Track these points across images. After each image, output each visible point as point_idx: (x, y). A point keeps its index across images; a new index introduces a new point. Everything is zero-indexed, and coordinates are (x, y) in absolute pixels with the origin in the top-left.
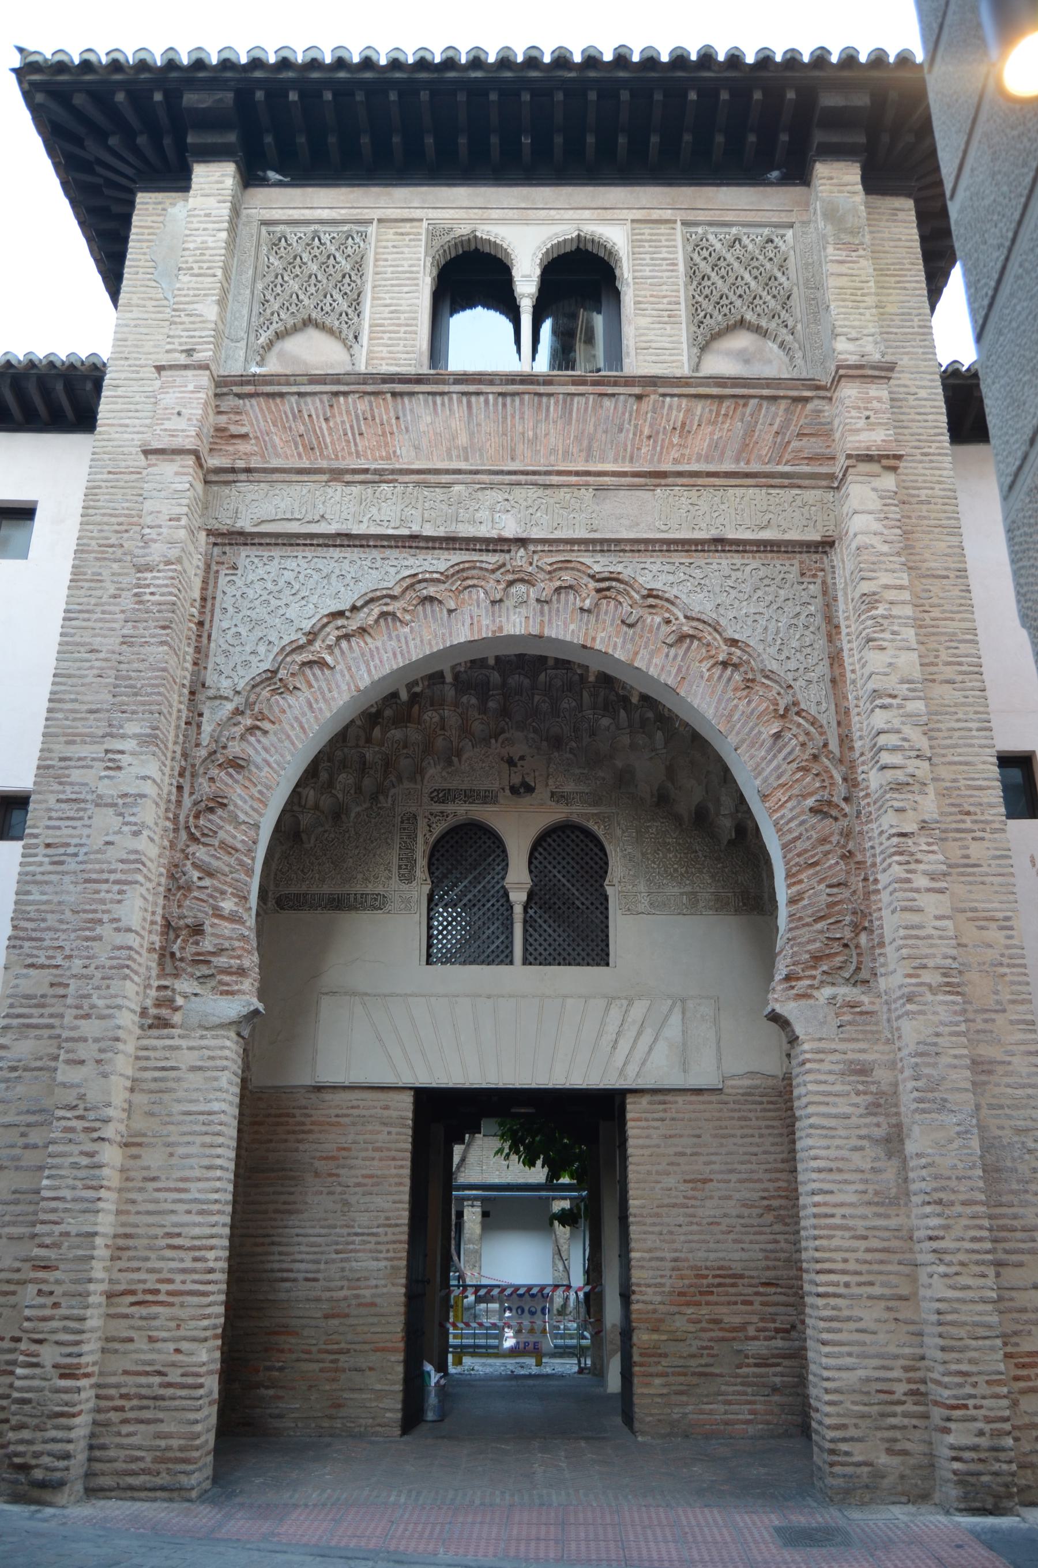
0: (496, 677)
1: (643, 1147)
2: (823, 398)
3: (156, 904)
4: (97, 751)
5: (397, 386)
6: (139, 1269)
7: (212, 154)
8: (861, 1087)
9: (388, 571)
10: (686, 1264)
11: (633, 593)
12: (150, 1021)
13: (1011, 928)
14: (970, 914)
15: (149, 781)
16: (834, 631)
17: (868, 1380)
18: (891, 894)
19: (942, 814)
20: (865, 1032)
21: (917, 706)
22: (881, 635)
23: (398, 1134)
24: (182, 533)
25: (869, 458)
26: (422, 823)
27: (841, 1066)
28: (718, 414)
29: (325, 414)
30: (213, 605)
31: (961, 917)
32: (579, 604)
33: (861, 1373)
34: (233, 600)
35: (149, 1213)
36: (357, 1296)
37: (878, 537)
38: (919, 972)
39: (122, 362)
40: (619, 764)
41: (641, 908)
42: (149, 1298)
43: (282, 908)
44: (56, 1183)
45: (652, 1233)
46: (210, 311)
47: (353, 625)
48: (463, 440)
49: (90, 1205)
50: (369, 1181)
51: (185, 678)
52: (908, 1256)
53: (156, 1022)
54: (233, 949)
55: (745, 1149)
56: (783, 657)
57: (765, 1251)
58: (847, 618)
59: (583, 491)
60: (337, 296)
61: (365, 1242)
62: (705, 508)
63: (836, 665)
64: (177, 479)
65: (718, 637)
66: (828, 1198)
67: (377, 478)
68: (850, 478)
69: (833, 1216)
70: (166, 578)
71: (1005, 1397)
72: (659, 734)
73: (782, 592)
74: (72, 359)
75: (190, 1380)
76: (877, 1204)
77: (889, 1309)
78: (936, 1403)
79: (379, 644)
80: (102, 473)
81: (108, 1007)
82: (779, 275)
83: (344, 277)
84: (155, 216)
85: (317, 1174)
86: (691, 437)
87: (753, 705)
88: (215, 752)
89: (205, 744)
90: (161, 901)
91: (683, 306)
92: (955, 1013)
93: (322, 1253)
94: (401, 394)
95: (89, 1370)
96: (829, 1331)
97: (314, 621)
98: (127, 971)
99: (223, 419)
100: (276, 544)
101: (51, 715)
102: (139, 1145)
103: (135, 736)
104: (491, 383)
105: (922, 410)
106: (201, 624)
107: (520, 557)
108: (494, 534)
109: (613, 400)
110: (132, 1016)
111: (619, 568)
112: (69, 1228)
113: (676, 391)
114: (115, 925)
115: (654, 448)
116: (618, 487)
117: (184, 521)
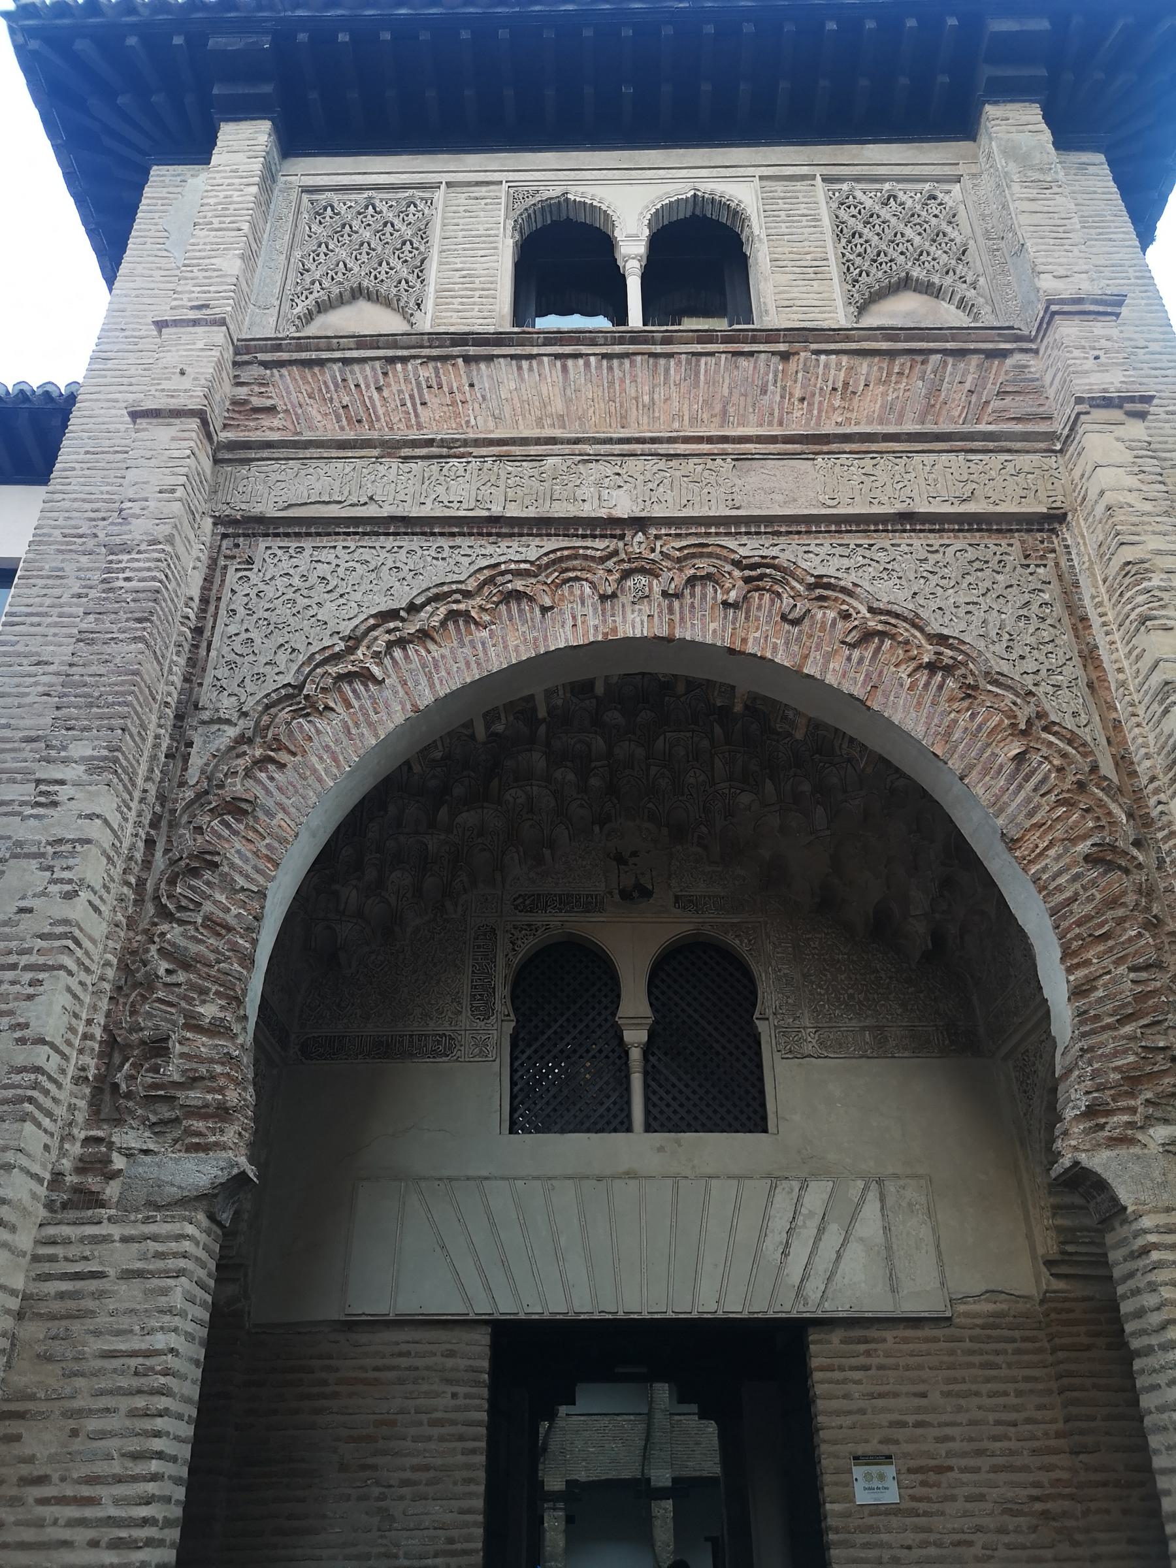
1: (838, 1413)
3: (95, 1008)
9: (463, 561)
15: (98, 822)
16: (1080, 626)
22: (1163, 613)
23: (467, 1396)
24: (177, 507)
25: (1106, 402)
28: (889, 375)
29: (376, 381)
30: (217, 608)
32: (720, 597)
34: (246, 599)
39: (117, 334)
41: (808, 1049)
46: (232, 265)
48: (558, 406)
51: (169, 694)
53: (76, 1197)
54: (213, 1077)
55: (997, 1416)
56: (1014, 656)
59: (719, 461)
64: (175, 445)
65: (918, 634)
67: (444, 451)
68: (1081, 431)
70: (148, 560)
72: (820, 810)
73: (1000, 578)
82: (949, 230)
83: (404, 243)
84: (173, 198)
85: (343, 1467)
86: (857, 398)
87: (979, 719)
88: (207, 793)
89: (192, 782)
90: (104, 1004)
91: (832, 261)
97: (356, 622)
98: (28, 1107)
99: (242, 392)
100: (308, 535)
102: (20, 1416)
103: (84, 760)
105: (1158, 365)
106: (198, 631)
107: (638, 542)
108: (603, 513)
109: (752, 360)
110: (33, 1185)
111: (774, 552)
114: (18, 1034)
116: (765, 457)
117: (178, 494)
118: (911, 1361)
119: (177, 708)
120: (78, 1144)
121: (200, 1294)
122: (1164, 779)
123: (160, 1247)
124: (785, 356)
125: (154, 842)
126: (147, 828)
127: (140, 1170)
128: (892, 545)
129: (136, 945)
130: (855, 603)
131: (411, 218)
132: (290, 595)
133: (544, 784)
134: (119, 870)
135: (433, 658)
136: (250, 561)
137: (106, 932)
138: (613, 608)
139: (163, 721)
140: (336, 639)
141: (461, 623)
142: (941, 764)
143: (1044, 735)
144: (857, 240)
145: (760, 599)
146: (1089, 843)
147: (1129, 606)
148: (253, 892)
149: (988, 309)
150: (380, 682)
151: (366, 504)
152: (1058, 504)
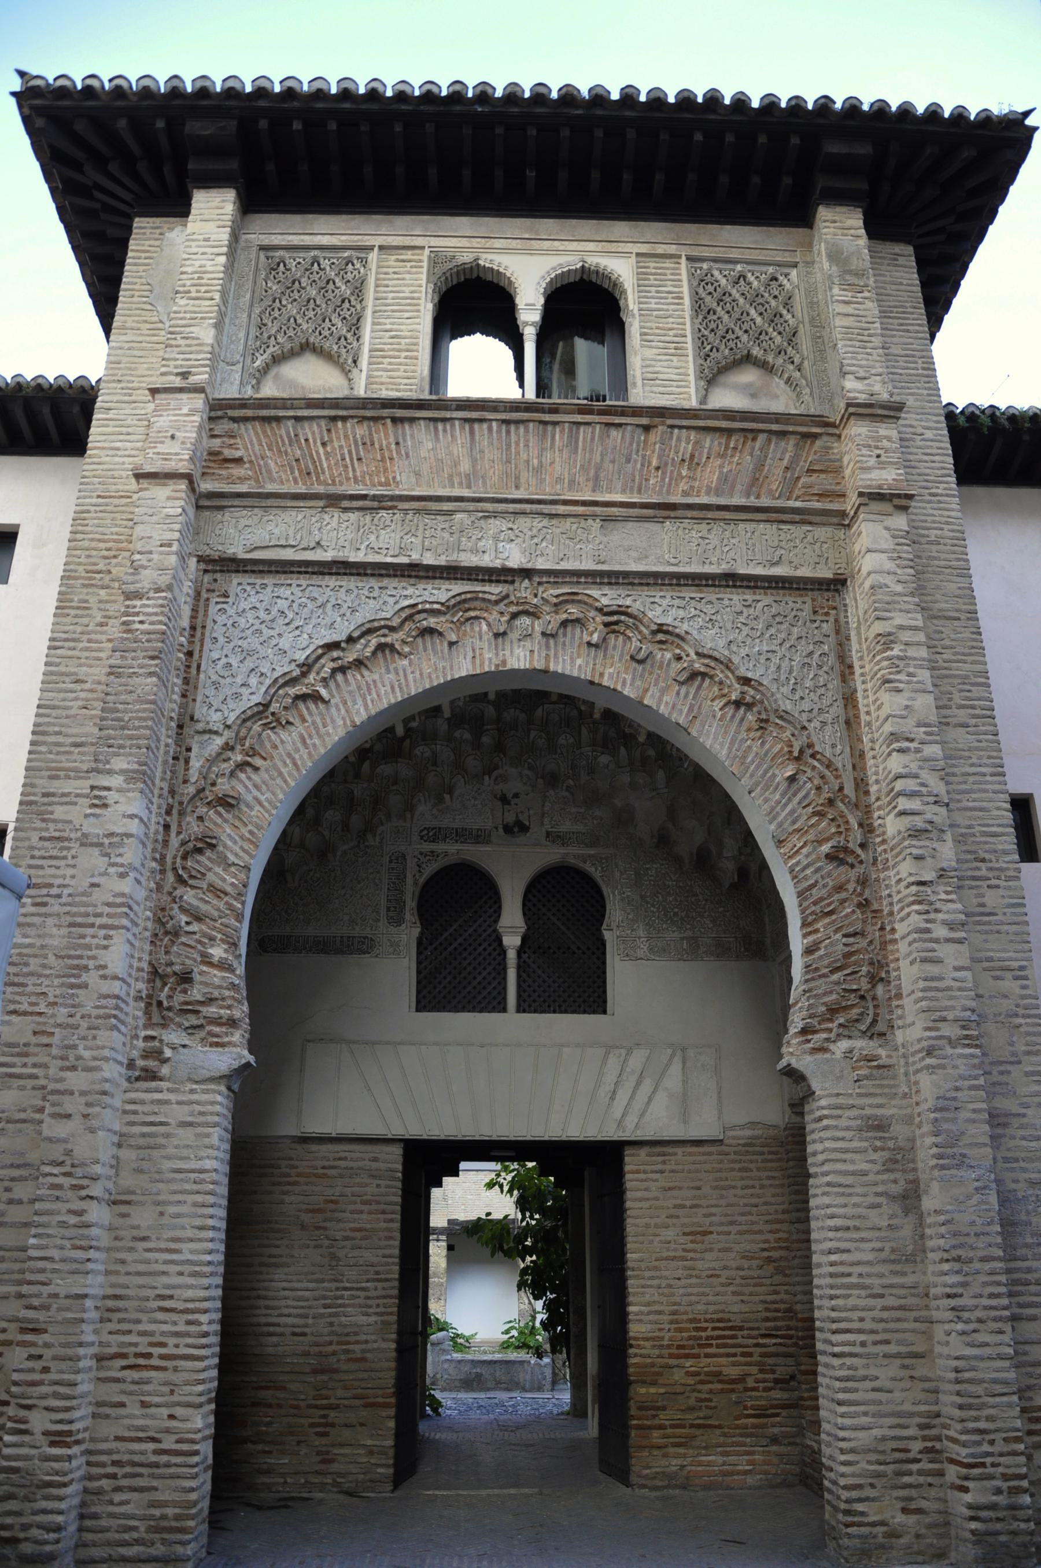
0: (490, 711)
1: (641, 1200)
2: (832, 435)
4: (83, 786)
5: (398, 412)
6: (130, 1332)
7: (212, 181)
8: (878, 1143)
10: (685, 1317)
11: (642, 628)
12: (137, 1074)
13: (1026, 978)
14: (986, 964)
15: (137, 820)
16: (847, 671)
17: (884, 1439)
18: (910, 944)
19: (958, 861)
20: (882, 1086)
21: (933, 750)
22: (898, 677)
23: (387, 1187)
24: (173, 559)
26: (411, 863)
27: (859, 1122)
28: (727, 448)
29: (322, 438)
30: (203, 634)
31: (978, 967)
32: (586, 638)
33: (876, 1432)
35: (139, 1274)
36: (347, 1352)
37: (891, 577)
38: (940, 1025)
39: (115, 385)
40: (618, 803)
41: (640, 953)
42: (141, 1361)
43: (265, 951)
44: (43, 1242)
45: (651, 1286)
46: (207, 334)
47: (351, 657)
48: (465, 466)
49: (78, 1266)
50: (358, 1235)
51: (173, 710)
52: (923, 1313)
53: (143, 1074)
54: (223, 999)
56: (797, 697)
57: (765, 1302)
58: (861, 658)
59: (590, 521)
60: (336, 320)
61: (354, 1297)
62: (715, 542)
63: (850, 707)
64: (169, 504)
66: (845, 1257)
68: (861, 516)
69: (849, 1275)
70: (155, 606)
71: (1022, 1454)
73: (795, 630)
74: (61, 382)
75: (185, 1447)
76: (893, 1262)
77: (904, 1367)
78: (952, 1461)
79: (376, 677)
80: (91, 497)
81: (95, 1059)
82: (785, 312)
83: (343, 301)
85: (303, 1227)
87: (767, 746)
88: (204, 789)
89: (193, 780)
90: (148, 947)
91: (689, 339)
92: (974, 1066)
93: (310, 1307)
94: (402, 420)
95: (80, 1436)
96: (845, 1390)
97: (308, 652)
98: (113, 1021)
99: (217, 442)
100: (270, 572)
101: (35, 748)
103: (122, 772)
104: (495, 409)
106: (190, 654)
107: (523, 590)
108: (497, 564)
109: (621, 430)
110: (119, 1068)
111: (628, 602)
112: (58, 1290)
113: (685, 423)
114: (101, 973)
115: (663, 479)
116: (626, 519)
118: (692, 1167)
124: (647, 429)
130: (686, 647)
131: (349, 276)
134: (149, 850)
140: (293, 665)
143: (810, 760)
144: (711, 317)
146: (829, 845)
149: (808, 391)
150: (326, 702)
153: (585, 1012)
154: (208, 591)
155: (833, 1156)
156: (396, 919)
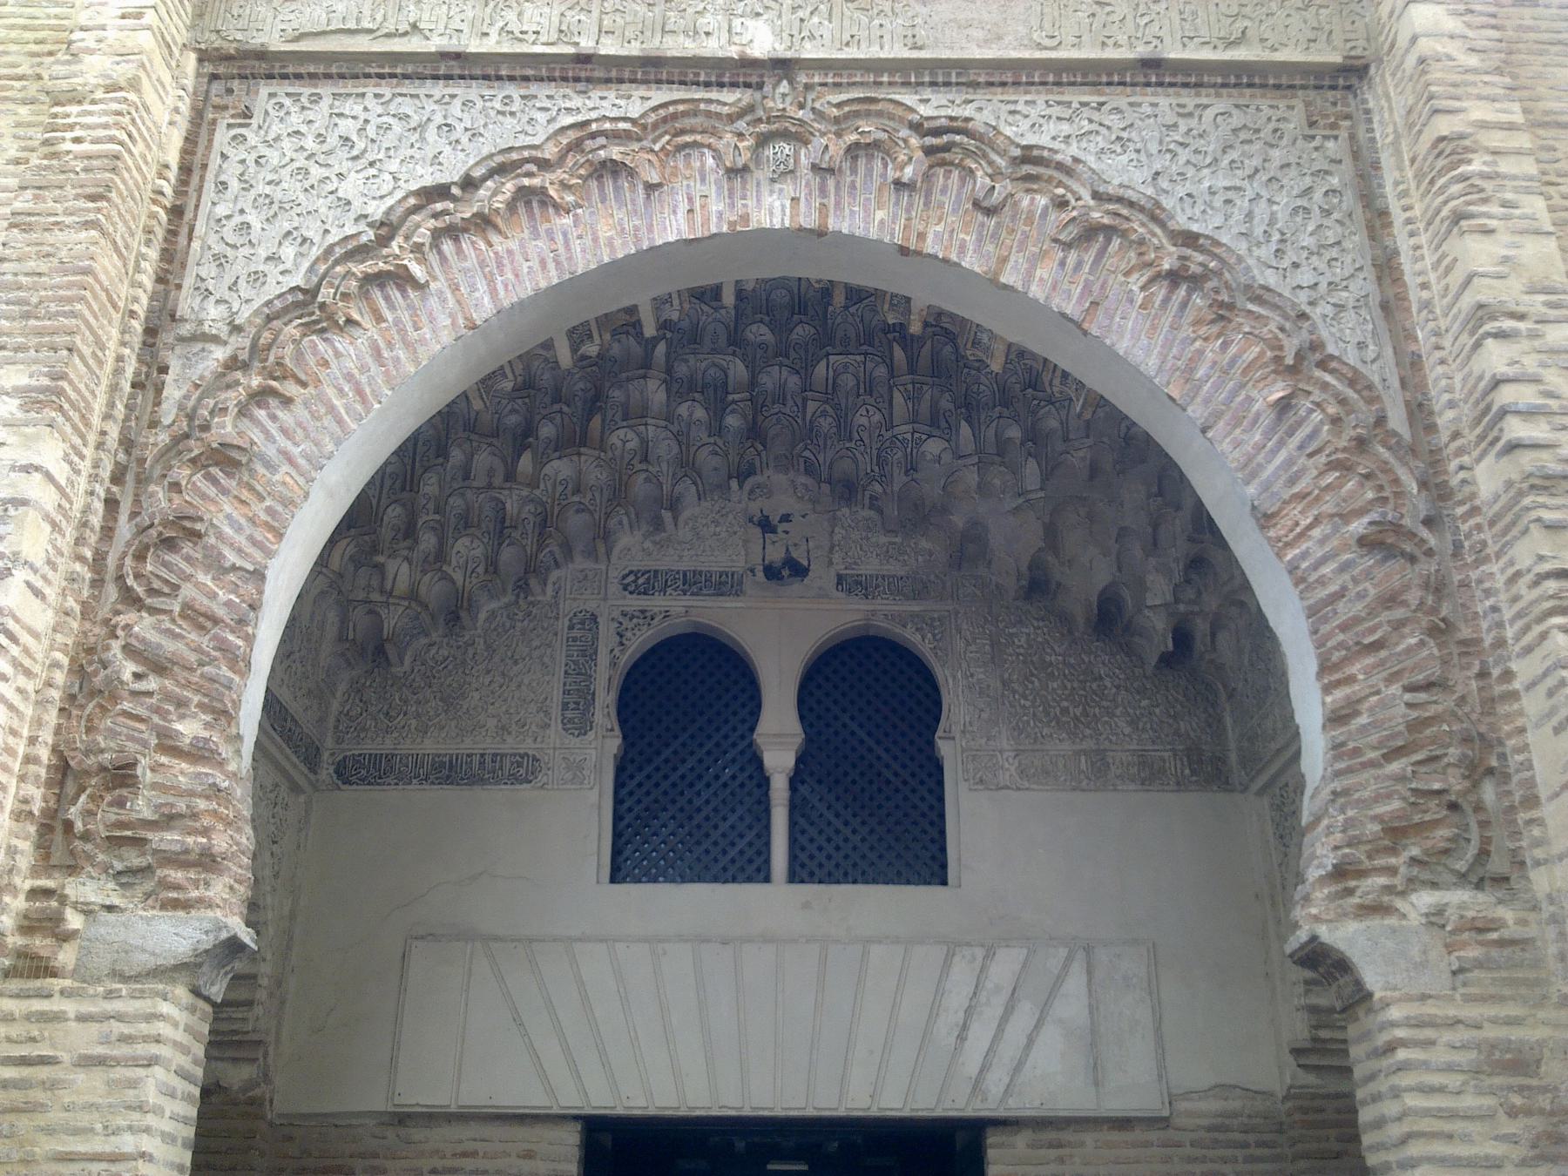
3: (38, 723)
8: (1517, 1100)
9: (536, 119)
15: (37, 476)
16: (1378, 224)
18: (1551, 693)
20: (1512, 982)
22: (1484, 209)
24: (146, 40)
26: (606, 632)
27: (1473, 1055)
30: (202, 179)
32: (892, 174)
34: (240, 168)
37: (1458, 43)
40: (958, 520)
43: (347, 782)
51: (136, 300)
53: (20, 963)
54: (195, 816)
56: (1286, 263)
65: (1158, 231)
70: (106, 113)
73: (1276, 154)
87: (1233, 350)
88: (187, 436)
89: (166, 421)
90: (52, 718)
97: (390, 202)
100: (328, 76)
103: (18, 391)
106: (176, 212)
108: (733, 52)
111: (968, 111)
117: (144, 21)
119: (147, 318)
120: (22, 897)
121: (181, 1086)
122: (1471, 436)
123: (126, 1029)
125: (117, 502)
126: (107, 483)
127: (102, 931)
128: (1131, 104)
129: (92, 640)
130: (1075, 186)
132: (301, 162)
133: (663, 423)
135: (496, 253)
136: (247, 114)
137: (52, 622)
138: (744, 188)
139: (127, 337)
140: (362, 227)
141: (535, 204)
142: (1178, 410)
143: (1318, 373)
145: (947, 178)
146: (1366, 520)
147: (1441, 199)
148: (247, 571)
151: (406, 34)
152: (1358, 52)
153: (908, 882)
154: (216, 107)
155: (1426, 1125)
156: (578, 721)
